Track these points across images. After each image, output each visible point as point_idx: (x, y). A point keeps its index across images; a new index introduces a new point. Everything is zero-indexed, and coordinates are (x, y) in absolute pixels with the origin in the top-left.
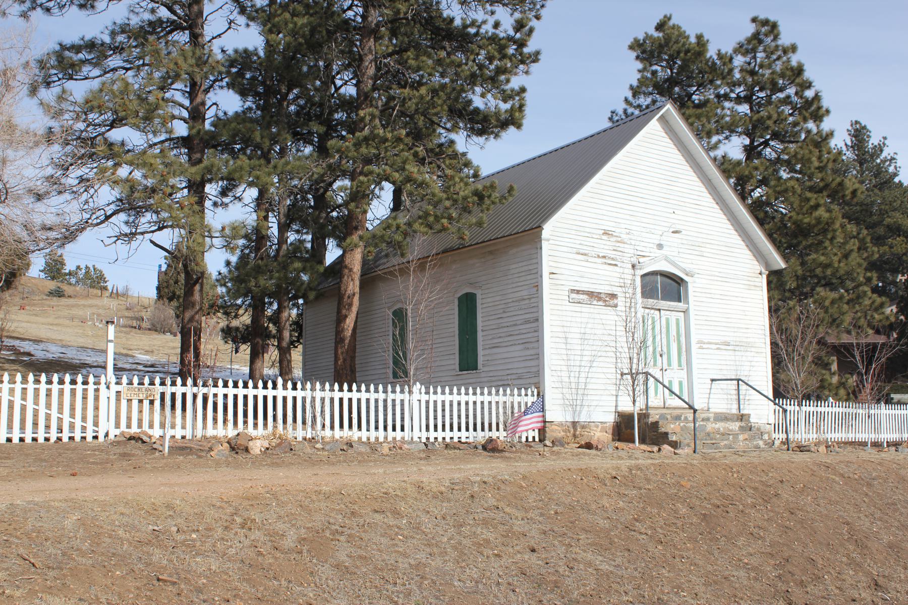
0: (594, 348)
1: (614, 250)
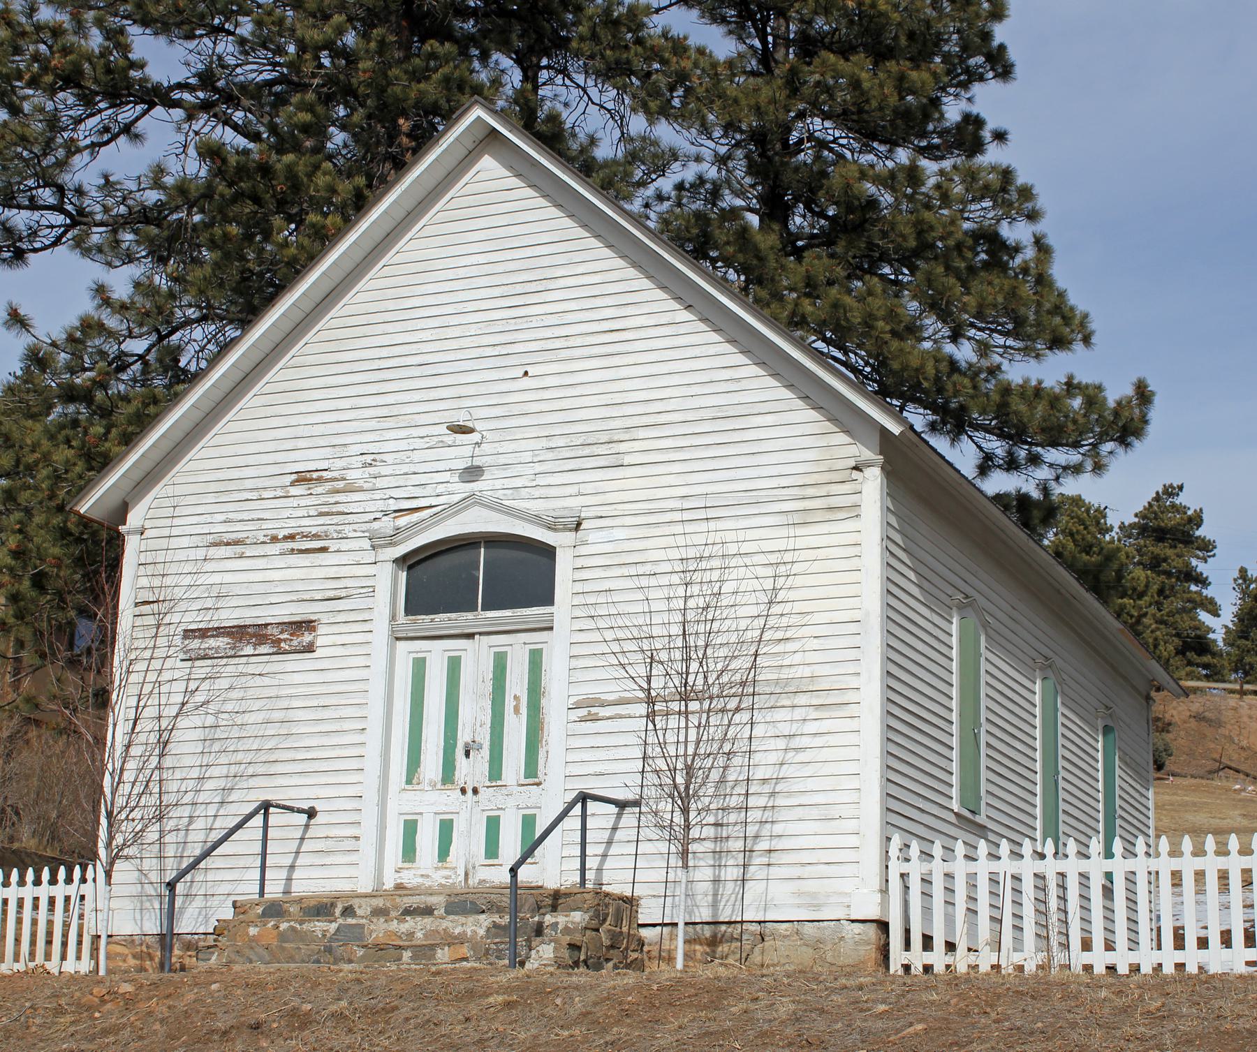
0: (240, 757)
1: (321, 514)
